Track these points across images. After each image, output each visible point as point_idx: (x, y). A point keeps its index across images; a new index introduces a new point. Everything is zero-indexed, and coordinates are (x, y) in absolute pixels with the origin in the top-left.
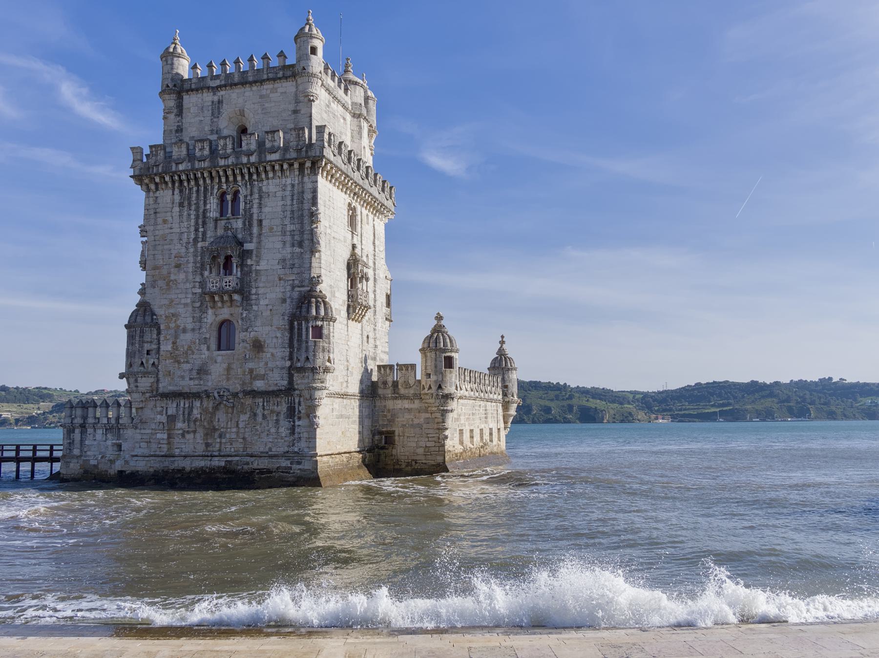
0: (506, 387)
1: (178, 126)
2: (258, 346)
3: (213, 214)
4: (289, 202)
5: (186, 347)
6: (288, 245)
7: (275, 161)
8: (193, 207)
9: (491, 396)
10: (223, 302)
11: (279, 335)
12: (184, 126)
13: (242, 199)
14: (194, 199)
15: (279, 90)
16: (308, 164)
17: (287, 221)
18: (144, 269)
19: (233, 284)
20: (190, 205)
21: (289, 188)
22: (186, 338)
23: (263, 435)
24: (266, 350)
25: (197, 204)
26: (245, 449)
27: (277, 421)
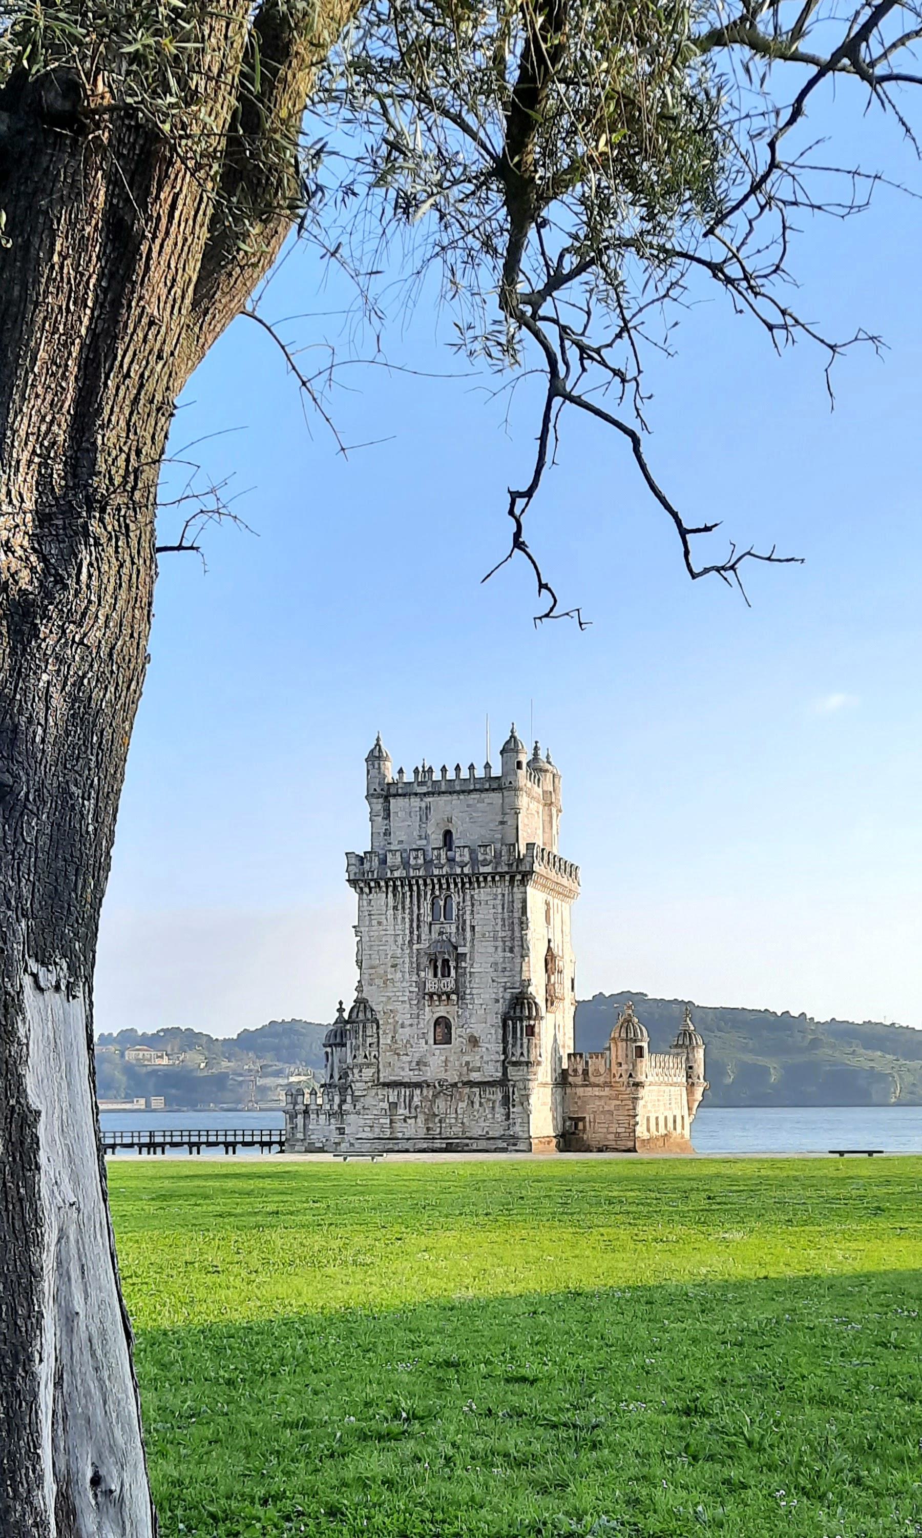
0: (691, 1068)
2: (474, 1041)
4: (500, 911)
6: (500, 949)
8: (407, 911)
9: (675, 1079)
10: (440, 1001)
13: (454, 906)
16: (519, 877)
17: (498, 928)
18: (360, 968)
19: (452, 985)
20: (403, 908)
21: (500, 897)
22: (404, 1034)
25: (411, 908)
26: (464, 1132)
27: (493, 1108)
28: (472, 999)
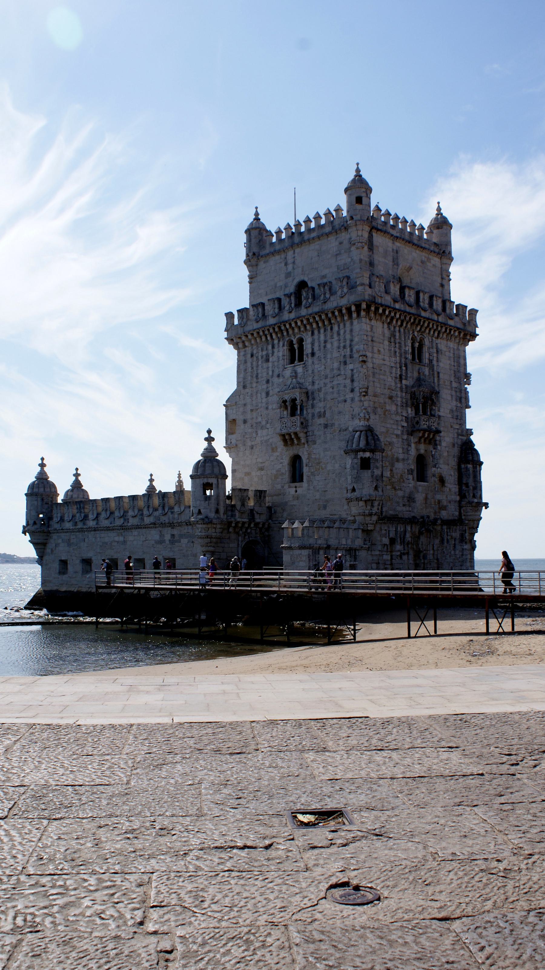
1: (371, 260)
2: (442, 481)
3: (410, 357)
4: (453, 363)
5: (399, 475)
7: (454, 327)
8: (397, 345)
11: (452, 473)
12: (376, 262)
14: (397, 337)
15: (432, 262)
16: (468, 337)
17: (452, 379)
21: (452, 351)
23: (448, 556)
24: (446, 485)
28: (440, 441)
